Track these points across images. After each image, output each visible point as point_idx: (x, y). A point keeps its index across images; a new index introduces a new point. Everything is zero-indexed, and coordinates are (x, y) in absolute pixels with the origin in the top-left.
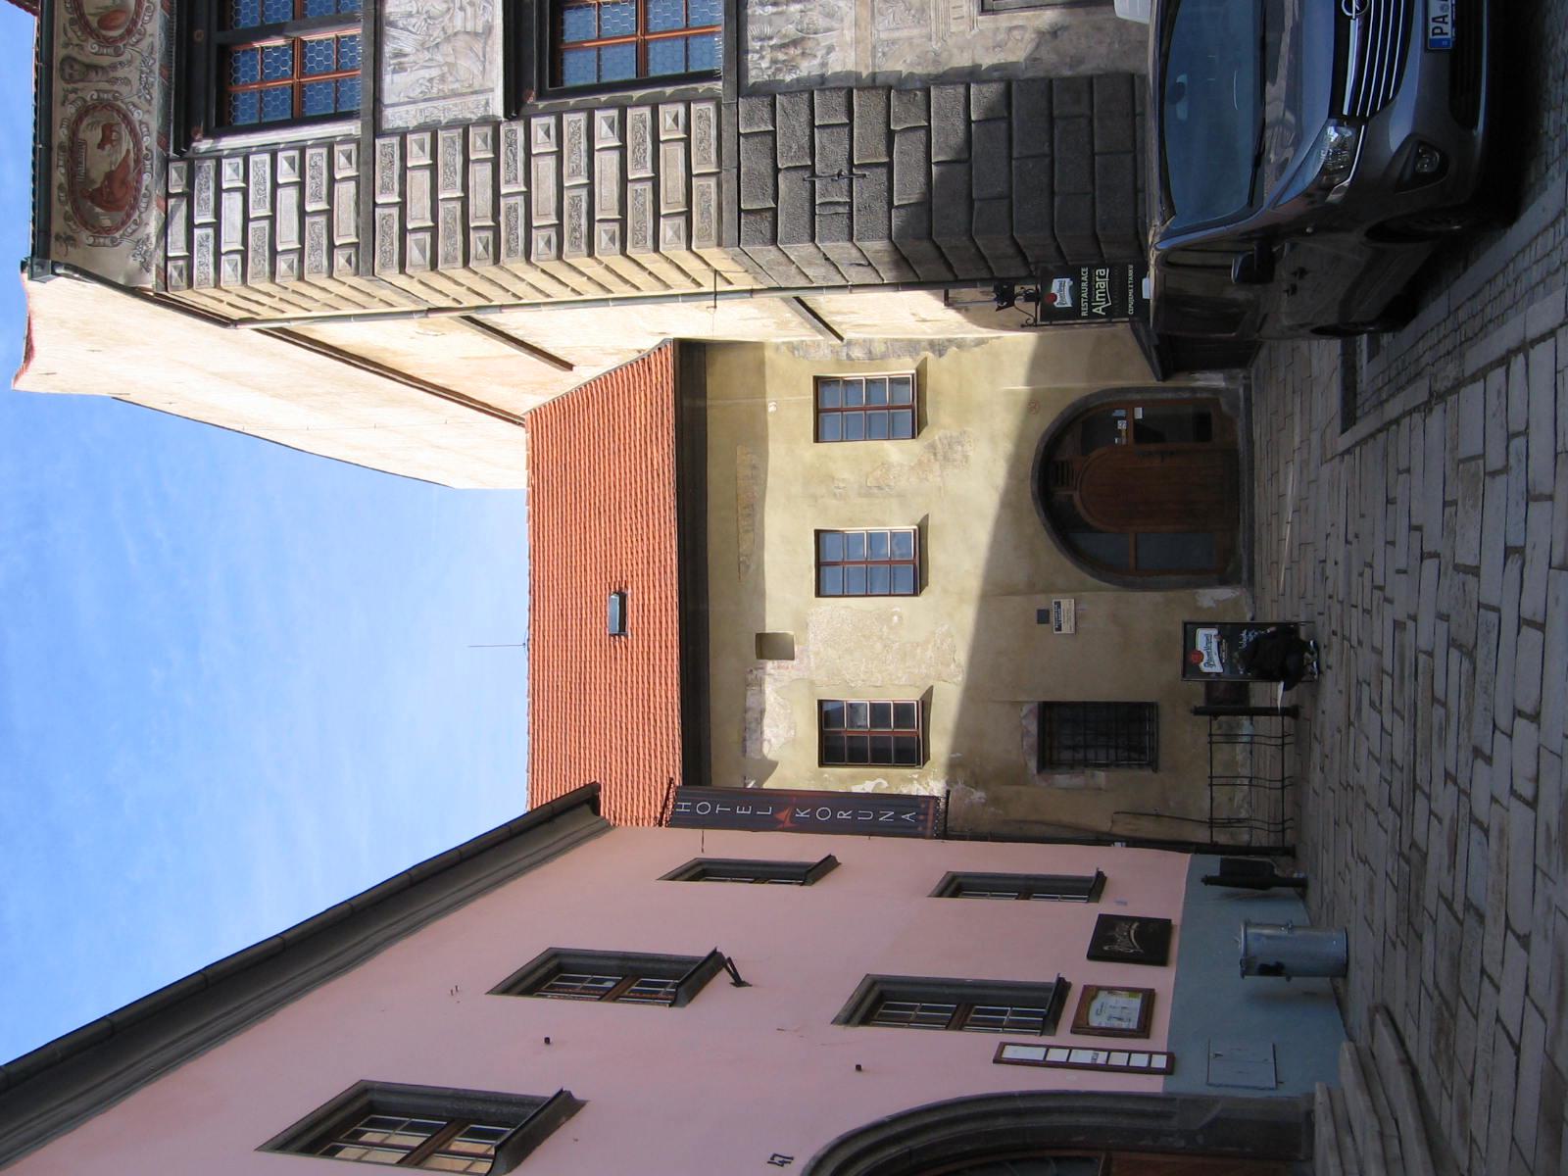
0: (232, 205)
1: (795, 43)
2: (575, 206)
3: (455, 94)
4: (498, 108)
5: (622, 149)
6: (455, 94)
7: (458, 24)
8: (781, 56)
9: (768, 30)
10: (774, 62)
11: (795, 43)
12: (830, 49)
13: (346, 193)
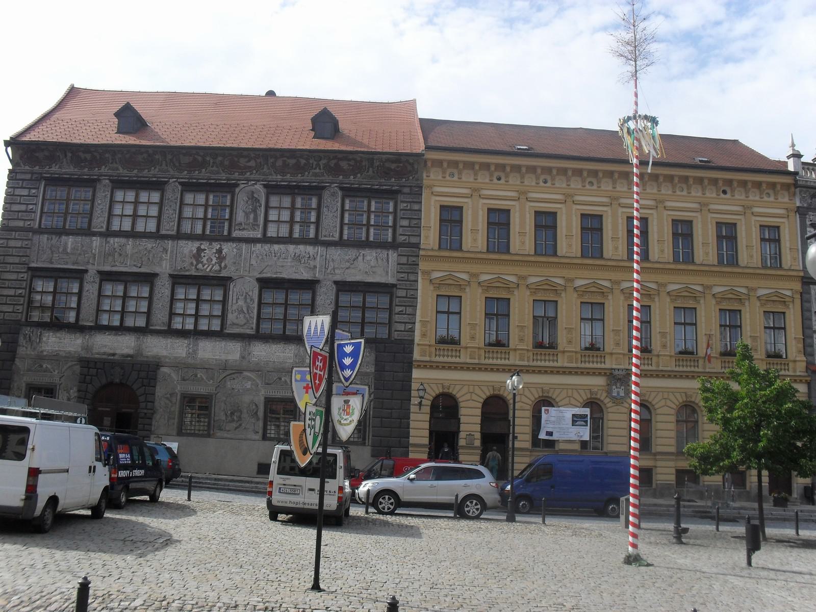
0: (25, 192)
1: (30, 339)
3: (38, 253)
4: (33, 265)
5: (15, 296)
6: (38, 253)
7: (55, 255)
8: (27, 336)
9: (34, 333)
10: (27, 334)
11: (30, 339)
12: (26, 348)
13: (21, 224)
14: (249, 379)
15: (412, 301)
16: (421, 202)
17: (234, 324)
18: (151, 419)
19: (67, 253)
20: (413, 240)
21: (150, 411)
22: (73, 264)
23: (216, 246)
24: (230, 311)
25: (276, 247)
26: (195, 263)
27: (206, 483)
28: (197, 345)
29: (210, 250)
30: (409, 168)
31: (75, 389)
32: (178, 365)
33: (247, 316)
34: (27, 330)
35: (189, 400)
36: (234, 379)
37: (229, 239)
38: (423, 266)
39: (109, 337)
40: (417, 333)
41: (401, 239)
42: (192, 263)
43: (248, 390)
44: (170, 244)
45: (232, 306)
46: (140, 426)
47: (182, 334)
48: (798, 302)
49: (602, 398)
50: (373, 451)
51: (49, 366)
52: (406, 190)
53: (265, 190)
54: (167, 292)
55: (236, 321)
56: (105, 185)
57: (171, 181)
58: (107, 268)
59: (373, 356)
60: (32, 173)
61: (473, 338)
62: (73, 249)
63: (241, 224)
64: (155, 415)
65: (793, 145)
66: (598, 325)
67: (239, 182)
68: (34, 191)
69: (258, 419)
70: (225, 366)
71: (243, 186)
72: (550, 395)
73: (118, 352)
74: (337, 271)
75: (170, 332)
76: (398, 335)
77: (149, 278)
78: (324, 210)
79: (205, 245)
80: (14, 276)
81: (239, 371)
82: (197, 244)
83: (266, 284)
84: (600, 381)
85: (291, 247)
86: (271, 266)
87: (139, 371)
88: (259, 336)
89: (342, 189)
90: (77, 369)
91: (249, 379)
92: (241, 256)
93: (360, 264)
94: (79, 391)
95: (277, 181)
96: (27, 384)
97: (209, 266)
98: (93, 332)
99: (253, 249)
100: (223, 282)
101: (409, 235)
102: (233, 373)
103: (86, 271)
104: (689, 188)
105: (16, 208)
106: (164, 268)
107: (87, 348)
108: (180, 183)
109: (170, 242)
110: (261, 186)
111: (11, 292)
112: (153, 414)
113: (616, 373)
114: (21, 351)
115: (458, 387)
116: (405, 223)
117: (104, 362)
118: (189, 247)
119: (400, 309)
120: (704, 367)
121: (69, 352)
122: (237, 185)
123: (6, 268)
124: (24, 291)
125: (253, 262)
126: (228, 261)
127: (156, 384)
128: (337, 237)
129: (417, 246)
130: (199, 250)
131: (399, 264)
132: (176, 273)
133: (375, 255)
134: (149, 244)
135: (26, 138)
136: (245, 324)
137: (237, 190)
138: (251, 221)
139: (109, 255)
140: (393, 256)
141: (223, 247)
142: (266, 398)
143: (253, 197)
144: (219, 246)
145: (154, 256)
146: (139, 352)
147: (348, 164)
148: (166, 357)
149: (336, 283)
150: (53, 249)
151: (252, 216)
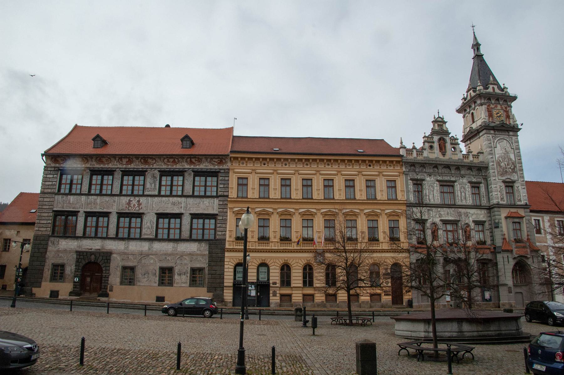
0: (51, 176)
1: (54, 243)
2: (42, 218)
4: (55, 209)
13: (50, 191)
14: (152, 258)
15: (225, 221)
16: (229, 176)
17: (145, 234)
18: (108, 278)
19: (70, 203)
20: (226, 194)
21: (108, 274)
22: (73, 208)
23: (137, 199)
24: (143, 228)
25: (164, 199)
26: (128, 207)
27: (130, 306)
28: (129, 244)
29: (134, 201)
30: (224, 161)
31: (74, 265)
32: (120, 253)
33: (151, 230)
34: (52, 239)
35: (124, 268)
36: (145, 259)
37: (143, 195)
38: (230, 205)
39: (89, 241)
40: (227, 236)
41: (220, 193)
42: (126, 207)
43: (152, 263)
44: (116, 198)
45: (144, 226)
46: (103, 281)
47: (123, 239)
49: (312, 263)
50: (207, 289)
51: (62, 255)
52: (222, 171)
53: (159, 173)
54: (116, 220)
55: (146, 233)
56: (87, 173)
57: (117, 170)
58: (89, 210)
59: (207, 247)
60: (55, 167)
61: (253, 237)
62: (73, 201)
63: (148, 189)
64: (110, 276)
65: (401, 143)
66: (310, 229)
67: (147, 170)
68: (55, 176)
69: (156, 277)
70: (141, 254)
71: (149, 171)
72: (288, 262)
73: (94, 248)
74: (191, 209)
75: (117, 238)
76: (219, 237)
77: (106, 215)
78: (186, 181)
79: (132, 199)
80: (46, 215)
81: (148, 255)
82: (129, 198)
83: (160, 216)
85: (171, 199)
86: (162, 207)
87: (103, 256)
88: (156, 239)
89: (193, 171)
90: (75, 256)
91: (152, 258)
92: (148, 203)
93: (201, 205)
94: (76, 266)
95: (164, 169)
96: (52, 264)
97: (134, 209)
98: (82, 239)
99: (154, 200)
100: (139, 215)
101: (223, 192)
102: (144, 256)
103: (79, 212)
104: (353, 165)
105: (47, 183)
106: (114, 210)
107: (79, 247)
108: (121, 171)
109: (117, 197)
110: (157, 171)
111: (45, 222)
112: (109, 276)
113: (318, 251)
114: (50, 248)
115: (269, 260)
116: (222, 186)
117: (87, 252)
118: (124, 200)
119: (220, 225)
120: (382, 247)
121: (71, 249)
122: (146, 171)
123: (43, 211)
124: (51, 221)
125: (155, 207)
126: (142, 206)
127: (110, 262)
128: (191, 194)
129: (227, 196)
130: (130, 201)
131: (219, 205)
132: (119, 211)
133: (208, 201)
134: (107, 198)
135: (51, 152)
136: (150, 234)
137: (147, 173)
138: (153, 187)
139: (89, 204)
140: (216, 201)
141: (140, 199)
142: (160, 267)
143: (154, 176)
144: (138, 199)
145: (109, 204)
146: (103, 247)
147: (195, 160)
148: (115, 250)
149: (191, 214)
150: (64, 202)
151: (153, 185)
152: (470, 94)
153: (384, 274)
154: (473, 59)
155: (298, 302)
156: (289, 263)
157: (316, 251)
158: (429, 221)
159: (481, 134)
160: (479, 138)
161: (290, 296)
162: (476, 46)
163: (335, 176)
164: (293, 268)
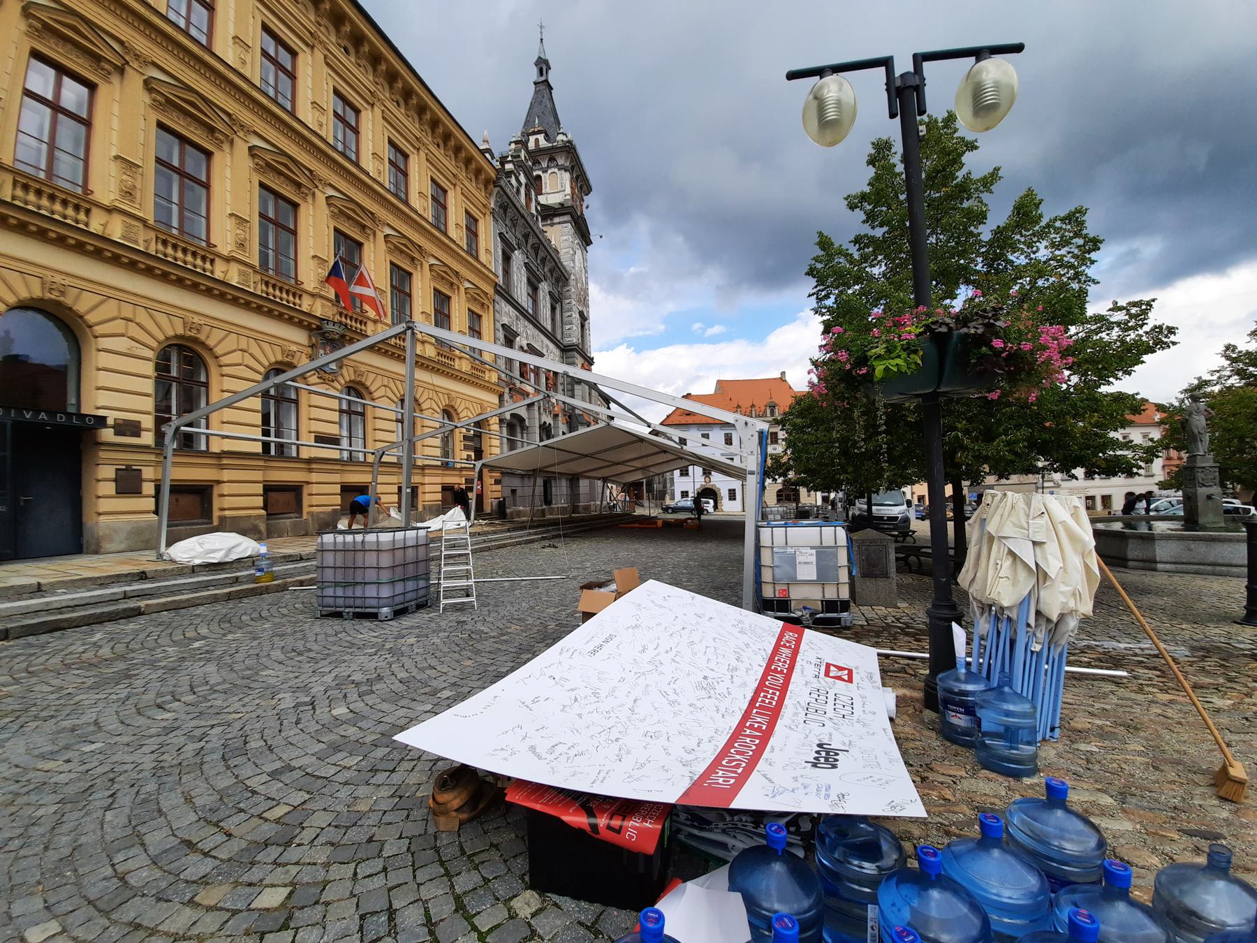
48: (491, 308)
72: (202, 337)
84: (299, 337)
152: (537, 140)
153: (466, 438)
154: (535, 83)
155: (249, 517)
156: (203, 344)
157: (319, 328)
158: (518, 339)
159: (556, 220)
160: (552, 225)
161: (295, 490)
162: (543, 65)
163: (365, 105)
164: (226, 370)
